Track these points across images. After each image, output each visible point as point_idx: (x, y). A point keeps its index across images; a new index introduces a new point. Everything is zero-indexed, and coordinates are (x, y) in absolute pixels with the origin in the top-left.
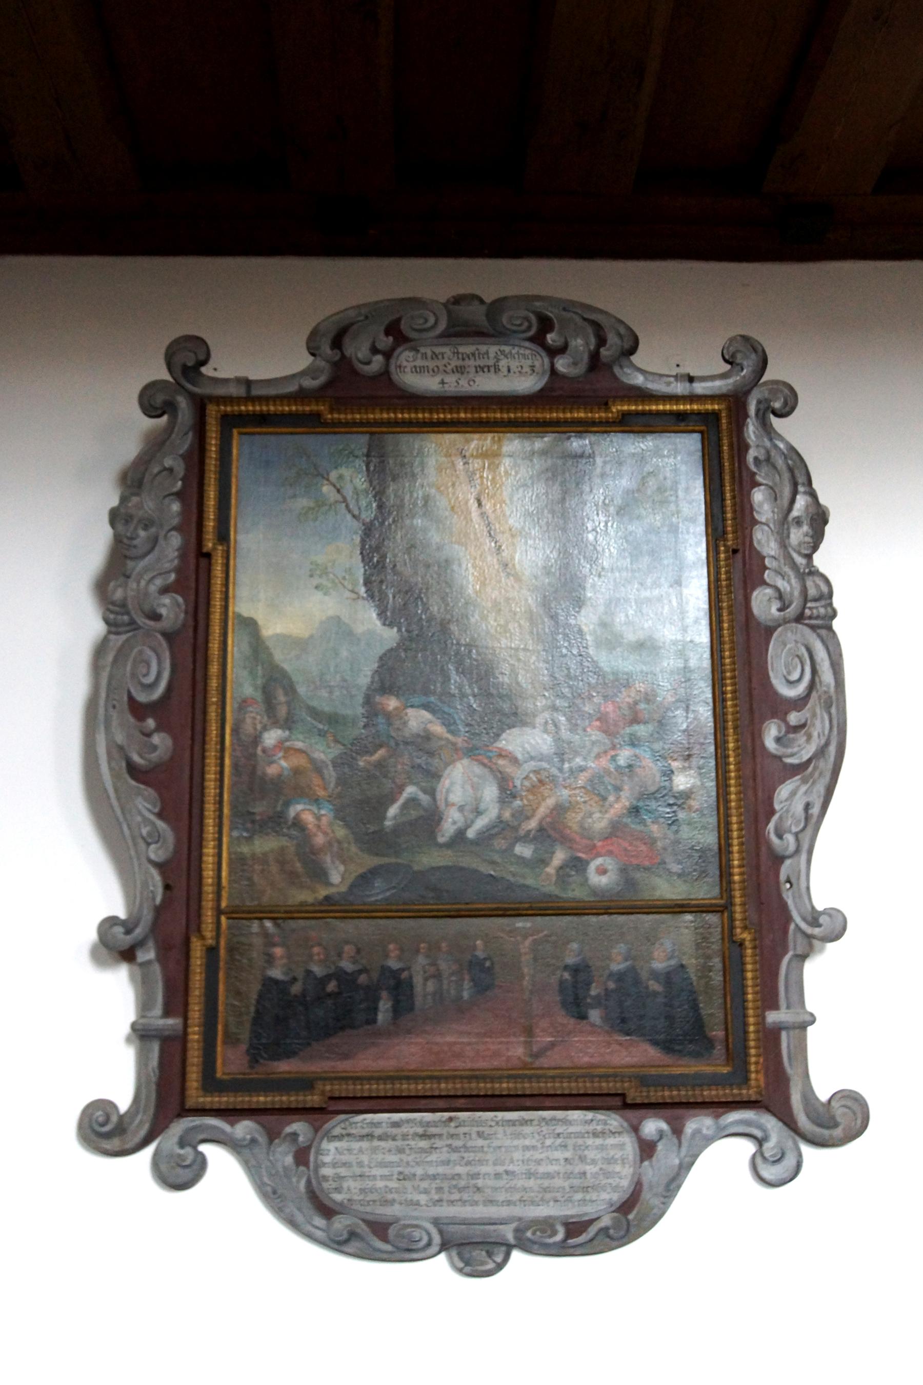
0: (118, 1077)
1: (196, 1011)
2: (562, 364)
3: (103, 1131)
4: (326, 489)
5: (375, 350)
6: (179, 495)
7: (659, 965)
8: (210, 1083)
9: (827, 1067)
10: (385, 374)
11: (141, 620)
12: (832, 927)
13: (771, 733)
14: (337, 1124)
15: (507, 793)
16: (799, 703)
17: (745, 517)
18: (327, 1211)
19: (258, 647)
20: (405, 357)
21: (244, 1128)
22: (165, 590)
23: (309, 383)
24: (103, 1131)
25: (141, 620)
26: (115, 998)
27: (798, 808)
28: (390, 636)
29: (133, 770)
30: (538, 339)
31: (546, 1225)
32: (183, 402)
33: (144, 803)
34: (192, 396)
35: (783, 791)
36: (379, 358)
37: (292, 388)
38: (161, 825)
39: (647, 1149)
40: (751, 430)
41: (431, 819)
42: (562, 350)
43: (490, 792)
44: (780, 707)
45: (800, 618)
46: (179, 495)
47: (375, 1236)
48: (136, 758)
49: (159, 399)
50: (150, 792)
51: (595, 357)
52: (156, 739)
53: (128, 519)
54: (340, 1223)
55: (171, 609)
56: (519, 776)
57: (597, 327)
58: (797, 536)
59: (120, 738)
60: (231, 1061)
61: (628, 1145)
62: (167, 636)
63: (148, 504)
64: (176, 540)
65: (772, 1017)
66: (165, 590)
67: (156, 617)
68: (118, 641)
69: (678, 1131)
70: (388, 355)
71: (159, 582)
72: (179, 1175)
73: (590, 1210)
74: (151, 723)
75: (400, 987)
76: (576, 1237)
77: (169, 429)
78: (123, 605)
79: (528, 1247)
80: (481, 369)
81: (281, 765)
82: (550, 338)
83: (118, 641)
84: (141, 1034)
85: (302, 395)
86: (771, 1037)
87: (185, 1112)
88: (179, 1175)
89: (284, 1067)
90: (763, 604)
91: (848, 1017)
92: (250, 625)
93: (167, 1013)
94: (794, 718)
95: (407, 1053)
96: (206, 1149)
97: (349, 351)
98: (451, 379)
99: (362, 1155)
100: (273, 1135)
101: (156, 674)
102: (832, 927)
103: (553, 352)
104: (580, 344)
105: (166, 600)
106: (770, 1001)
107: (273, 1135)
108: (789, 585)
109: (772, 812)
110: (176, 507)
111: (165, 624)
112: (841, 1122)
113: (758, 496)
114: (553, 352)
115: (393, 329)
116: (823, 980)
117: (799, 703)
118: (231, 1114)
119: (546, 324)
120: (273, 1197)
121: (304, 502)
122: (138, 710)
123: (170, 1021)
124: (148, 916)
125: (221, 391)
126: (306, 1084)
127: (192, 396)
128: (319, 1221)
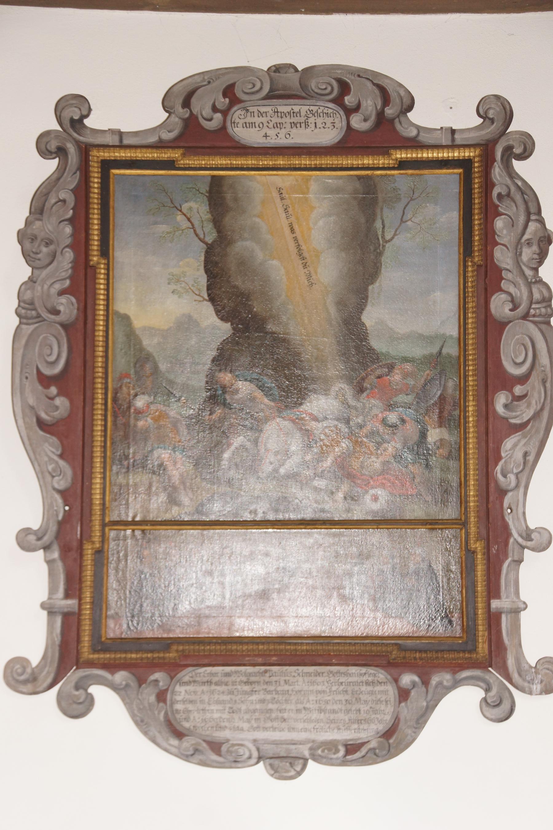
1: (87, 595)
2: (357, 122)
4: (180, 218)
5: (215, 109)
6: (71, 221)
10: (223, 128)
11: (45, 315)
13: (501, 400)
14: (186, 674)
16: (523, 379)
17: (490, 239)
18: (179, 734)
19: (131, 335)
20: (237, 114)
21: (121, 676)
22: (62, 293)
23: (167, 136)
24: (23, 679)
25: (45, 315)
27: (519, 455)
29: (41, 424)
30: (339, 101)
31: (331, 746)
32: (71, 149)
33: (51, 447)
34: (78, 143)
35: (508, 444)
36: (218, 116)
37: (153, 139)
38: (62, 463)
39: (404, 695)
40: (497, 172)
42: (357, 108)
44: (508, 382)
45: (525, 317)
46: (71, 221)
48: (43, 415)
49: (53, 146)
50: (54, 439)
51: (380, 115)
52: (58, 401)
53: (33, 238)
54: (188, 743)
55: (68, 307)
57: (383, 91)
58: (527, 254)
59: (31, 401)
61: (391, 691)
62: (64, 326)
63: (47, 226)
64: (69, 255)
65: (495, 604)
66: (62, 293)
67: (57, 312)
68: (28, 329)
69: (426, 683)
70: (225, 113)
71: (58, 287)
72: (77, 707)
73: (363, 736)
74: (53, 390)
77: (61, 170)
78: (32, 303)
79: (317, 759)
80: (294, 125)
82: (348, 100)
83: (28, 329)
85: (160, 145)
86: (493, 620)
87: (79, 665)
88: (77, 707)
90: (499, 306)
92: (126, 318)
93: (67, 595)
94: (518, 390)
96: (95, 690)
97: (196, 109)
98: (272, 132)
100: (141, 681)
101: (56, 355)
103: (349, 112)
104: (370, 104)
105: (63, 299)
107: (141, 681)
108: (521, 292)
109: (499, 458)
110: (68, 230)
111: (61, 318)
113: (499, 223)
114: (349, 112)
115: (229, 91)
117: (523, 379)
118: (111, 667)
119: (345, 88)
121: (163, 228)
122: (45, 381)
123: (69, 602)
124: (53, 528)
125: (99, 140)
127: (78, 143)
128: (175, 742)
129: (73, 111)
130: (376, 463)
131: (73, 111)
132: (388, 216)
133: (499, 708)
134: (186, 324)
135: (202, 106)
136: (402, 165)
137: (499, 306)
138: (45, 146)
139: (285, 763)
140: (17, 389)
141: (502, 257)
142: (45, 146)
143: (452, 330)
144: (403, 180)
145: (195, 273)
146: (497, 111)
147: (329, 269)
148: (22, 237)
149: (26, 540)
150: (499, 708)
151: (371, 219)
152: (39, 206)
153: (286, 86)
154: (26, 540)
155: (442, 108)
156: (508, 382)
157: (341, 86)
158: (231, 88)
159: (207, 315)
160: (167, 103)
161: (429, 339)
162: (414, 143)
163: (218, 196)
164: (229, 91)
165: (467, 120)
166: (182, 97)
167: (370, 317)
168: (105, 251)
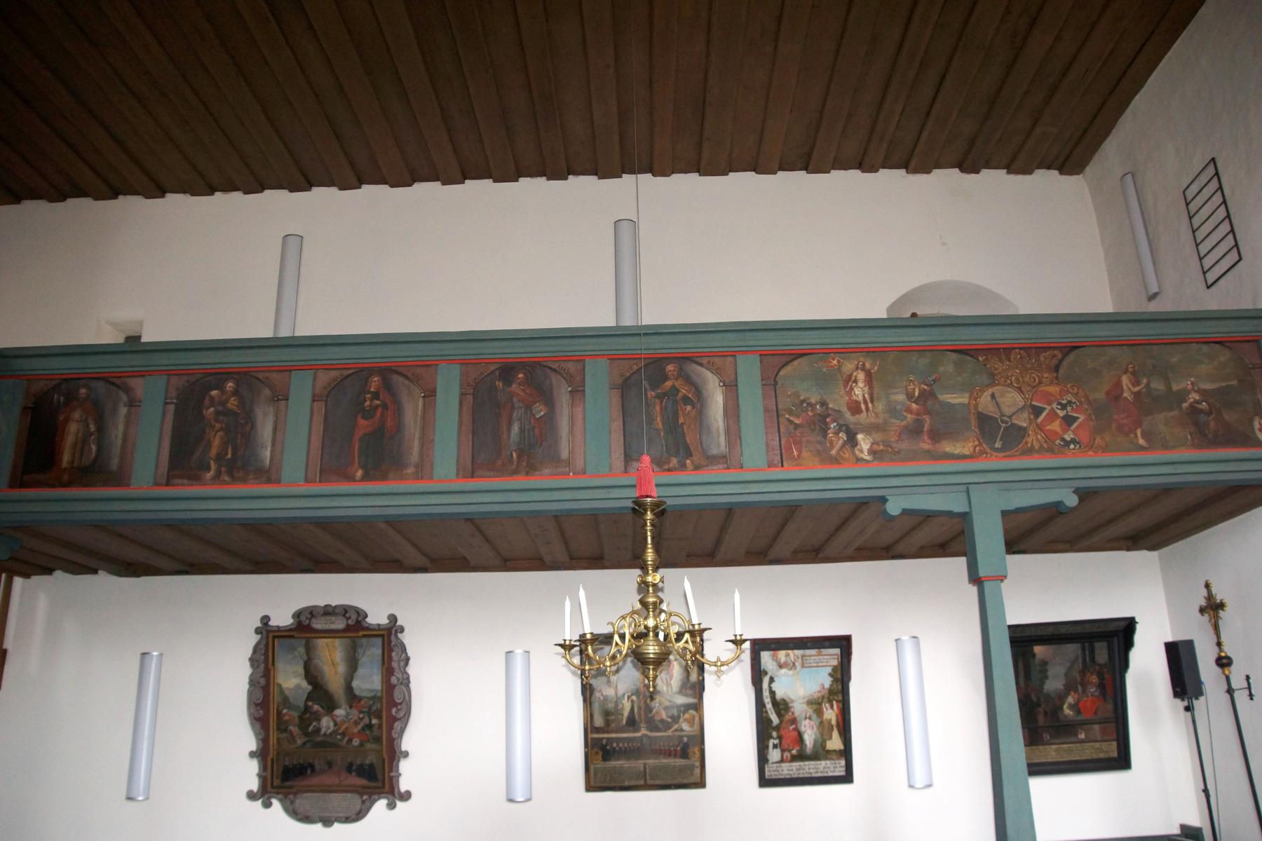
0: (254, 785)
1: (269, 771)
2: (350, 622)
3: (252, 796)
7: (368, 762)
8: (273, 787)
9: (404, 785)
12: (406, 754)
13: (394, 710)
15: (336, 724)
17: (390, 658)
20: (314, 620)
24: (252, 796)
26: (254, 766)
28: (310, 688)
33: (258, 725)
39: (363, 802)
40: (393, 638)
41: (318, 730)
43: (332, 724)
44: (396, 705)
47: (306, 819)
55: (263, 681)
56: (338, 720)
58: (402, 664)
60: (277, 782)
61: (360, 801)
72: (267, 805)
75: (312, 767)
76: (347, 820)
81: (286, 718)
84: (259, 775)
85: (291, 630)
86: (391, 779)
88: (267, 805)
89: (288, 784)
90: (394, 680)
91: (408, 774)
92: (279, 685)
95: (315, 780)
99: (304, 802)
101: (259, 695)
102: (406, 754)
103: (348, 619)
104: (354, 616)
106: (391, 770)
108: (400, 676)
112: (406, 796)
114: (348, 619)
115: (311, 613)
116: (404, 766)
119: (346, 612)
120: (287, 810)
122: (257, 705)
126: (291, 787)
129: (265, 620)
130: (356, 731)
131: (265, 620)
132: (360, 651)
133: (391, 806)
134: (298, 687)
135: (303, 618)
136: (364, 636)
137: (394, 680)
138: (258, 631)
139: (327, 822)
140: (249, 708)
141: (394, 665)
142: (258, 631)
143: (379, 688)
144: (364, 640)
145: (301, 670)
146: (393, 618)
147: (342, 668)
148: (251, 660)
149: (252, 754)
150: (391, 806)
151: (355, 652)
152: (255, 650)
153: (329, 611)
154: (252, 754)
155: (377, 617)
156: (396, 705)
157: (345, 611)
158: (312, 612)
159: (304, 684)
160: (294, 616)
161: (371, 691)
162: (367, 629)
163: (309, 649)
164: (311, 613)
165: (384, 621)
166: (297, 615)
167: (355, 684)
168: (273, 664)
